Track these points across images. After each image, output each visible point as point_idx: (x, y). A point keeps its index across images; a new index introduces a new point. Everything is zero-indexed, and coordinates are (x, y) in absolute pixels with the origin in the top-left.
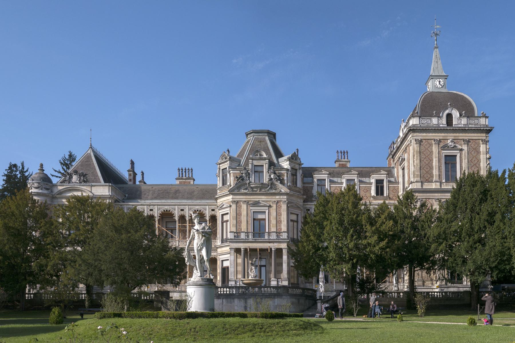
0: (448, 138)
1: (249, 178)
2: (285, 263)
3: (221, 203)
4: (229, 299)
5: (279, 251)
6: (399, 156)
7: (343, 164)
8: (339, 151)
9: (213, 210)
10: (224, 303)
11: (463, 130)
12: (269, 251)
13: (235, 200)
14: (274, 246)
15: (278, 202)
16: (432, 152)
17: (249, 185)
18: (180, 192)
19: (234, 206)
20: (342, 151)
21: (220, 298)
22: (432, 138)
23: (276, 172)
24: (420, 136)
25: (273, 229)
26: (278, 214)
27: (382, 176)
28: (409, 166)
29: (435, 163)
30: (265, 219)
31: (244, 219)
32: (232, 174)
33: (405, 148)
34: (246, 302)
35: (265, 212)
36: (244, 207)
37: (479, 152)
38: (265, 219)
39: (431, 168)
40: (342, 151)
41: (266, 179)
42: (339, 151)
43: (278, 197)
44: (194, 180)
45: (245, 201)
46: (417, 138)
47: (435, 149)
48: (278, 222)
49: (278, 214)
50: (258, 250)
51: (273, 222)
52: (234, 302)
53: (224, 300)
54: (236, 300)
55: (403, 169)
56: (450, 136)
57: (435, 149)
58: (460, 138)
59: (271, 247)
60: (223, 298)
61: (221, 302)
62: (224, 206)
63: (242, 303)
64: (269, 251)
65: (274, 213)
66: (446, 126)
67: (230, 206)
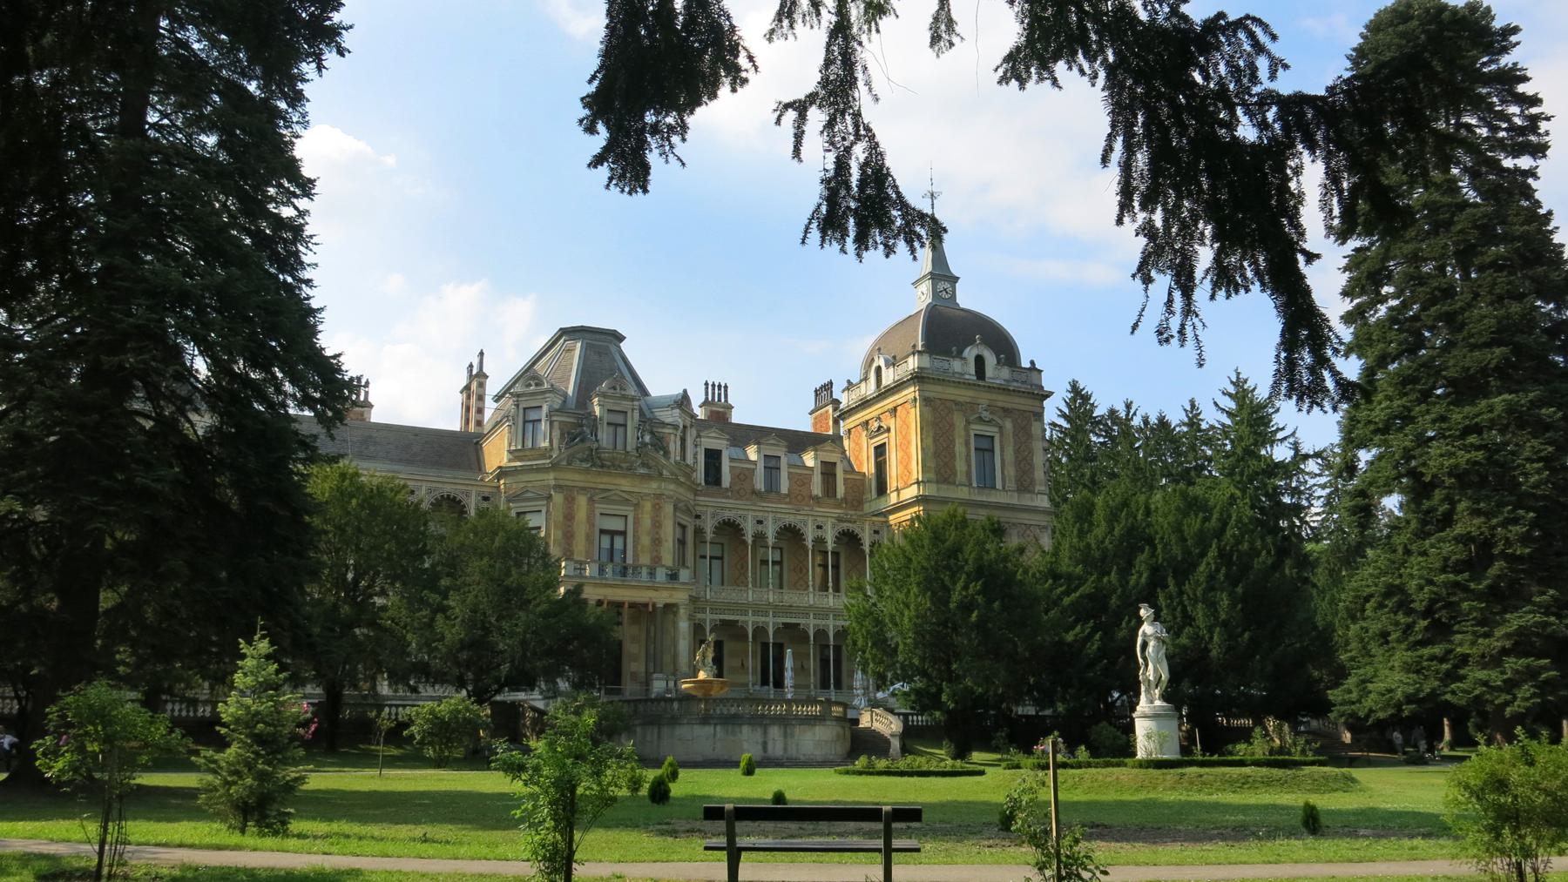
0: (980, 401)
1: (596, 436)
2: (685, 639)
3: (522, 485)
4: (730, 728)
5: (670, 608)
6: (867, 418)
7: (718, 412)
8: (710, 383)
9: (486, 499)
10: (718, 735)
11: (1003, 390)
12: (650, 609)
13: (561, 482)
14: (661, 598)
15: (659, 496)
16: (952, 426)
17: (597, 453)
18: (375, 443)
19: (558, 498)
20: (717, 384)
21: (709, 724)
22: (952, 398)
23: (655, 430)
24: (936, 391)
25: (645, 559)
26: (657, 525)
27: (833, 457)
28: (904, 446)
29: (959, 448)
30: (623, 533)
31: (581, 530)
32: (556, 425)
33: (891, 406)
34: (765, 733)
35: (626, 516)
36: (582, 501)
37: (1030, 436)
38: (623, 533)
39: (953, 457)
40: (717, 384)
41: (631, 444)
42: (710, 383)
43: (654, 485)
44: (371, 406)
45: (584, 489)
46: (927, 394)
47: (959, 421)
48: (657, 542)
49: (657, 525)
50: (627, 605)
51: (646, 540)
52: (741, 732)
53: (718, 728)
54: (746, 729)
55: (880, 450)
56: (984, 398)
57: (959, 421)
58: (1000, 404)
59: (655, 600)
60: (716, 724)
61: (712, 732)
62: (529, 495)
63: (758, 735)
64: (650, 609)
65: (647, 522)
66: (975, 378)
67: (549, 497)
